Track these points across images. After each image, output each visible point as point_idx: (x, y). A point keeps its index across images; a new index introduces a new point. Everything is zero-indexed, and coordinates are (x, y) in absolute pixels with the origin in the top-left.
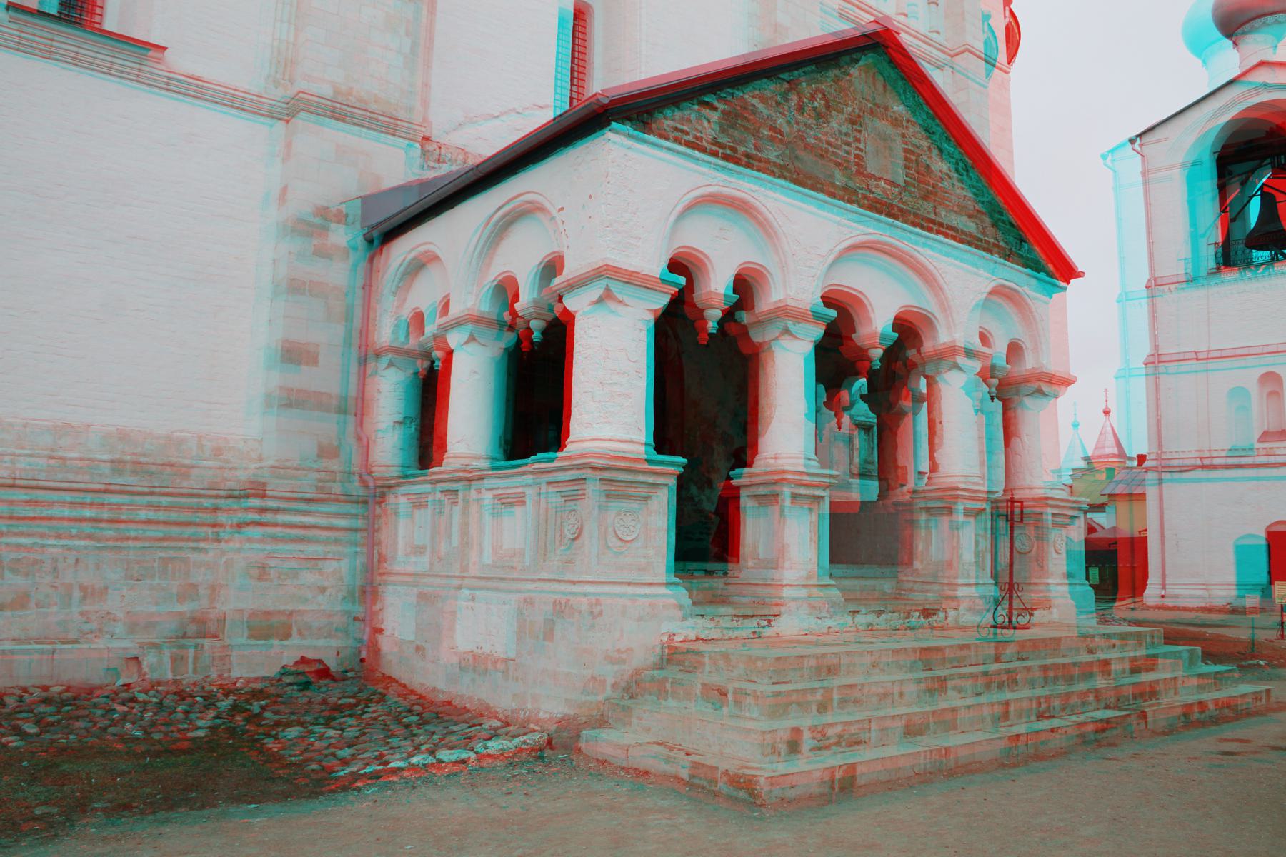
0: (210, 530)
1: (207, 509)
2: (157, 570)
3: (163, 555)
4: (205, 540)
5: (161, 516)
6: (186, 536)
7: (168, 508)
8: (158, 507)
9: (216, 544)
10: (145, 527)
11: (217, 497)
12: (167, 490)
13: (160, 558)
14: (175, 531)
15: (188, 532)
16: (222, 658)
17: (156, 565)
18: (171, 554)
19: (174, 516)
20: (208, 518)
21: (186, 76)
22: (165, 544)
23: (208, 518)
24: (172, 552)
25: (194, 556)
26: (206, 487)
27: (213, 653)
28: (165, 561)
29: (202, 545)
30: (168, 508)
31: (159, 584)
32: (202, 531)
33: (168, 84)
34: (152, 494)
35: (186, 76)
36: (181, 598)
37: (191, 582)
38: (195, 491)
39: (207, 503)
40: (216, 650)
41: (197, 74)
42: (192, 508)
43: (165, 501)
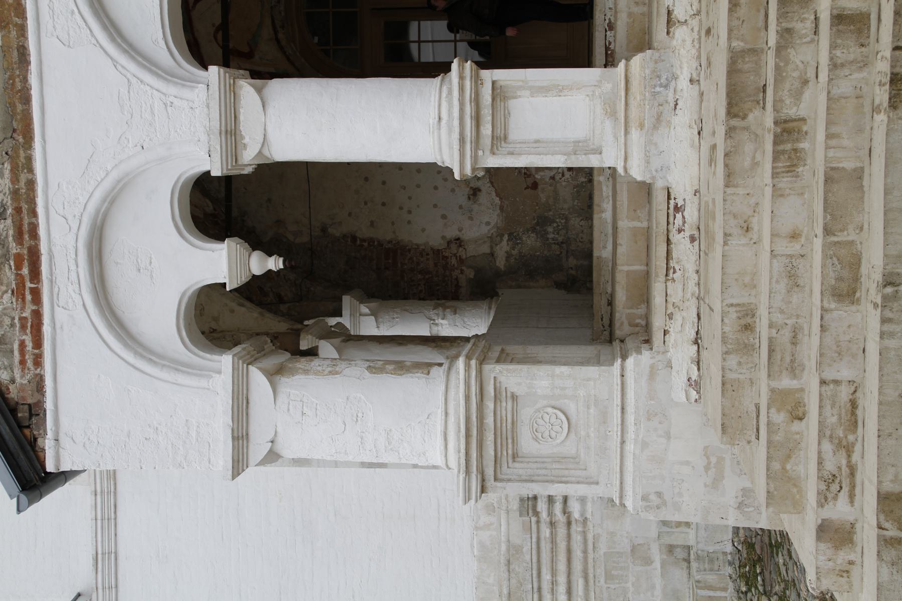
0: (574, 527)
1: (552, 533)
2: (618, 586)
3: (602, 580)
4: (584, 534)
5: (562, 579)
6: (582, 555)
7: (554, 573)
8: (554, 583)
9: (588, 523)
10: (574, 593)
11: (538, 522)
12: (535, 575)
13: (606, 582)
14: (577, 566)
15: (578, 553)
16: (711, 561)
17: (612, 586)
18: (600, 571)
19: (562, 567)
20: (561, 531)
21: (97, 573)
22: (591, 576)
23: (561, 531)
24: (598, 571)
25: (603, 548)
26: (529, 536)
27: (705, 570)
28: (609, 577)
29: (590, 536)
30: (554, 573)
31: (633, 585)
32: (577, 539)
33: (110, 588)
34: (539, 589)
35: (97, 573)
36: (648, 561)
37: (629, 550)
38: (534, 546)
39: (546, 532)
40: (702, 568)
41: (91, 562)
42: (552, 548)
43: (546, 576)
